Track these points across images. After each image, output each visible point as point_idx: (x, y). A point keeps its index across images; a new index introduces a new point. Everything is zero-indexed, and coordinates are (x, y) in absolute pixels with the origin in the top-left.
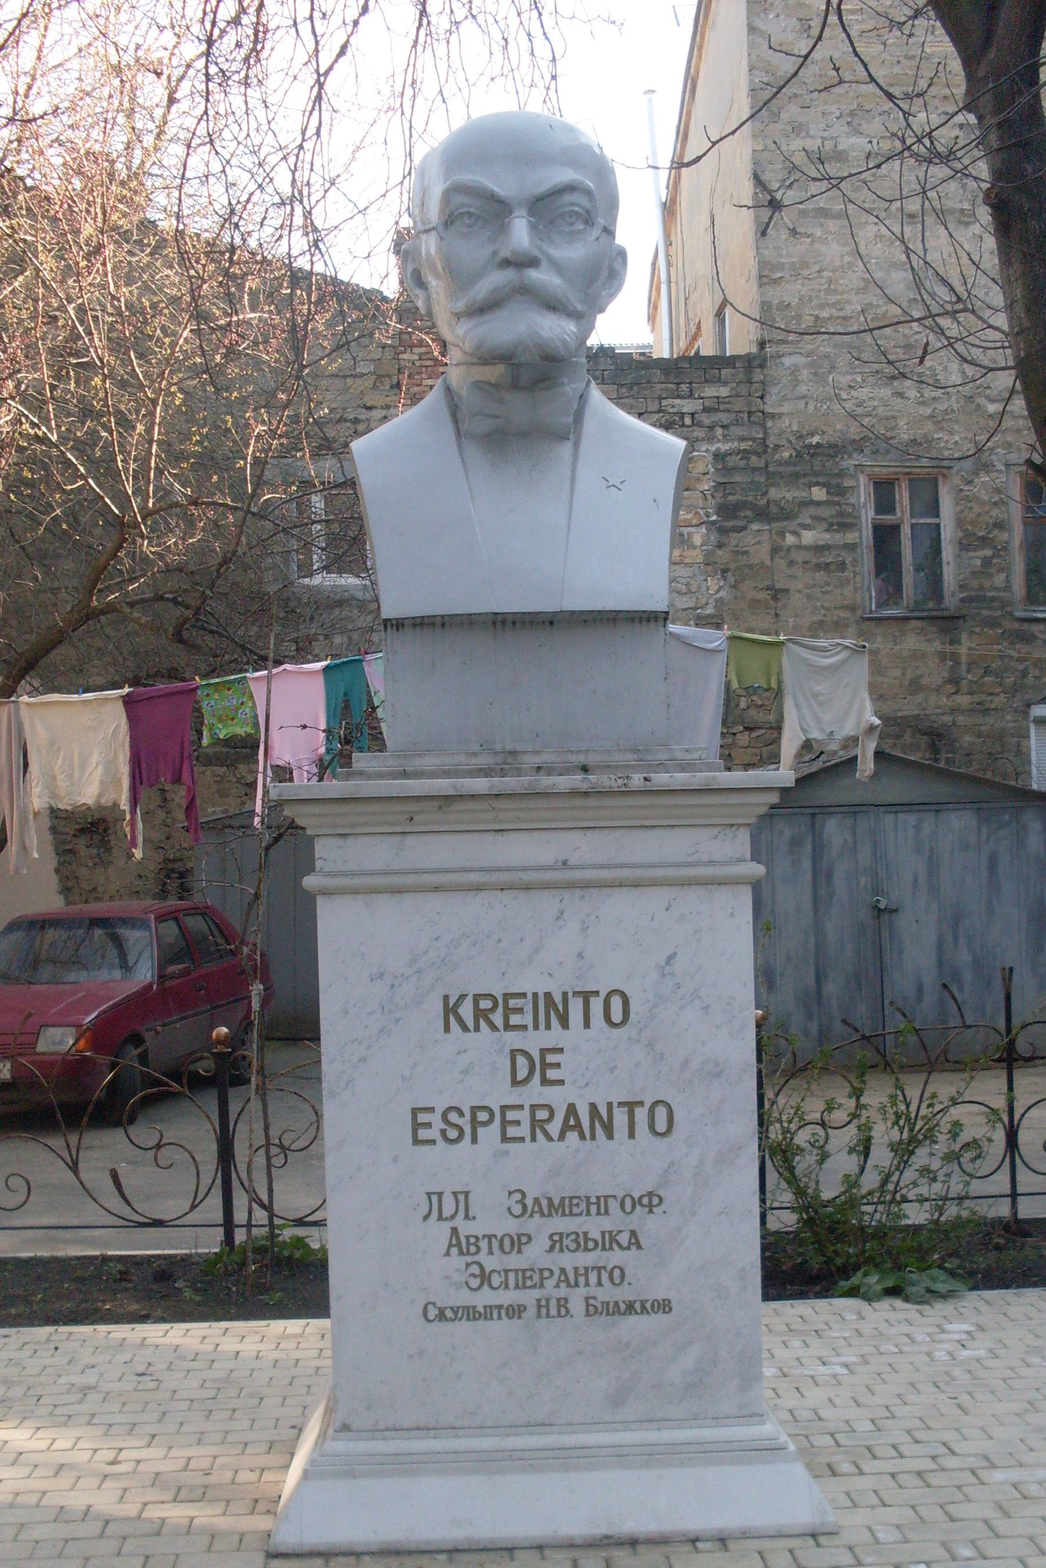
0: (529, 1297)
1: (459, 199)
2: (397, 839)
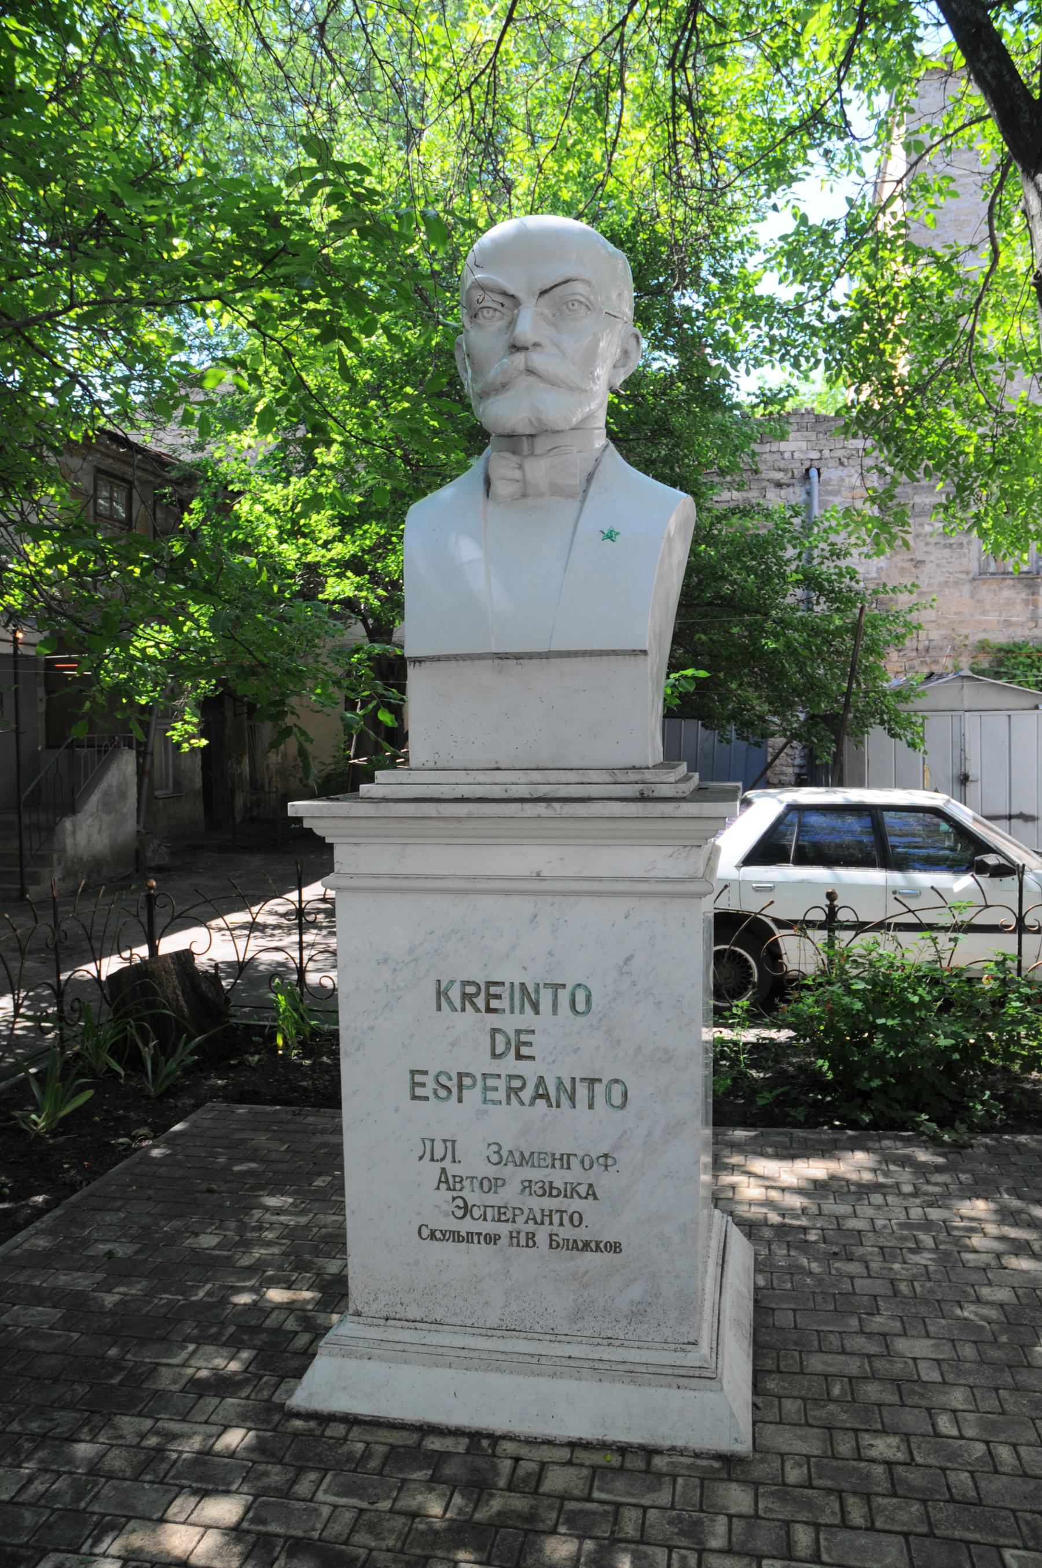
0: (504, 1229)
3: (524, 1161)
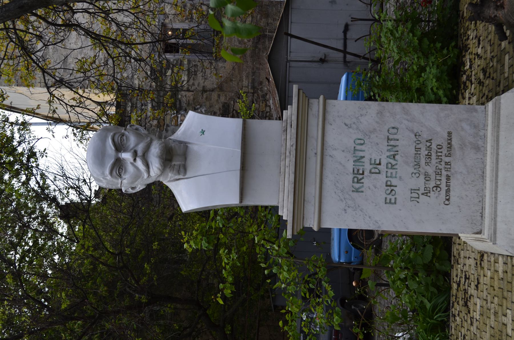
0: (444, 173)
1: (114, 173)
2: (305, 203)
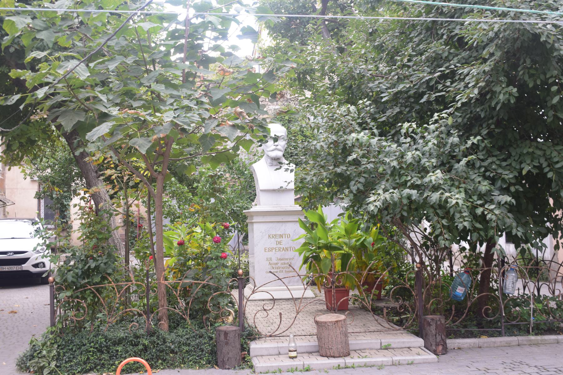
0: (279, 270)
3: (281, 260)
